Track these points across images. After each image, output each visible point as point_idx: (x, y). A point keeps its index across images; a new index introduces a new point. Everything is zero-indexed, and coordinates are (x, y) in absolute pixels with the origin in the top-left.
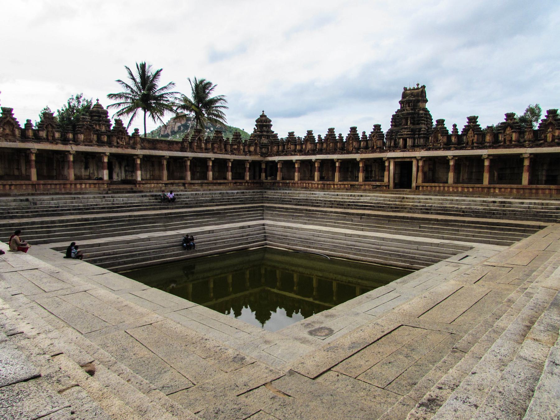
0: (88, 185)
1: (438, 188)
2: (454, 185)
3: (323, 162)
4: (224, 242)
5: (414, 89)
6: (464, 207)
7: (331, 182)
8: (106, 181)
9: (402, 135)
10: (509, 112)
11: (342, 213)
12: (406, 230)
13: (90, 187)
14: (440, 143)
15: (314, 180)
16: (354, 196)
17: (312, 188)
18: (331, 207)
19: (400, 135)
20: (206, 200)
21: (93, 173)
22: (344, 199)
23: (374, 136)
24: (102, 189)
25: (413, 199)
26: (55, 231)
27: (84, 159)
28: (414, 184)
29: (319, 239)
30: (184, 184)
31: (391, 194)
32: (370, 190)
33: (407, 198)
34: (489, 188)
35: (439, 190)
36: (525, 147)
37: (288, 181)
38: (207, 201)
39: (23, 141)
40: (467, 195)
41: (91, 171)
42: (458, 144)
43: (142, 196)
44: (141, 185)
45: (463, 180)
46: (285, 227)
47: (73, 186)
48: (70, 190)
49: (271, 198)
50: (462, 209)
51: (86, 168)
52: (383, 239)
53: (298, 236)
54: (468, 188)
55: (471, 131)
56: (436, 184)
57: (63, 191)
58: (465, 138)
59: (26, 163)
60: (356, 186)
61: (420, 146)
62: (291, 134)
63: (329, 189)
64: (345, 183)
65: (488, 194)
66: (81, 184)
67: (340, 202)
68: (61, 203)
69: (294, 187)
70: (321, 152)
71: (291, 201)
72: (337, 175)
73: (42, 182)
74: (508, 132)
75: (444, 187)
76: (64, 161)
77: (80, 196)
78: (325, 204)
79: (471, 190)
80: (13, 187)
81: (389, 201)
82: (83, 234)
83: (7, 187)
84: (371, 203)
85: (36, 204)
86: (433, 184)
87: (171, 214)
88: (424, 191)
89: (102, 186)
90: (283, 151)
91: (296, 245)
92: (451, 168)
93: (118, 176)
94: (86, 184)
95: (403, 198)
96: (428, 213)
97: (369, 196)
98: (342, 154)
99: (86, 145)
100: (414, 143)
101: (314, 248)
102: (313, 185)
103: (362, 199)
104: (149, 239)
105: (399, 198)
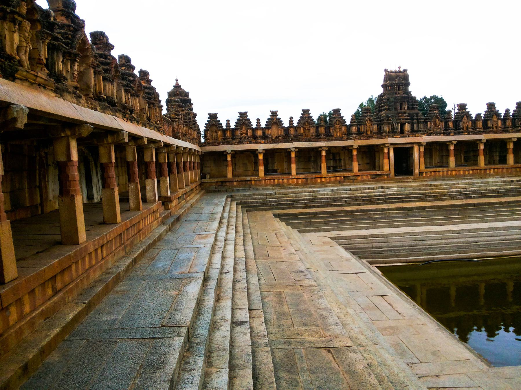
1: (441, 173)
2: (457, 168)
3: (300, 151)
5: (396, 72)
6: (495, 188)
7: (318, 175)
9: (400, 119)
10: (491, 101)
11: (397, 209)
12: (487, 217)
14: (440, 129)
15: (290, 174)
16: (373, 188)
17: (289, 184)
18: (359, 204)
19: (397, 120)
22: (364, 193)
23: (367, 120)
25: (441, 185)
28: (417, 171)
29: (429, 242)
31: (397, 182)
32: (369, 181)
33: (434, 185)
34: (486, 169)
35: (443, 175)
36: (509, 133)
37: (249, 178)
40: (471, 177)
42: (456, 129)
45: (435, 163)
46: (365, 237)
49: (251, 203)
50: (493, 190)
52: (496, 229)
53: (398, 244)
54: (468, 170)
55: (465, 118)
56: (441, 169)
58: (461, 123)
60: (351, 178)
61: (420, 131)
62: (243, 115)
63: (314, 184)
64: (337, 174)
65: (486, 175)
67: (362, 197)
69: (260, 185)
70: (297, 138)
71: (293, 204)
72: (324, 166)
74: (495, 119)
75: (447, 171)
78: (346, 201)
79: (471, 172)
81: (420, 190)
84: (402, 194)
86: (438, 169)
88: (429, 177)
90: (233, 139)
91: (410, 255)
92: (452, 153)
95: (431, 186)
96: (470, 198)
97: (391, 187)
98: (328, 140)
100: (412, 128)
101: (436, 254)
102: (291, 181)
103: (388, 191)
105: (426, 186)
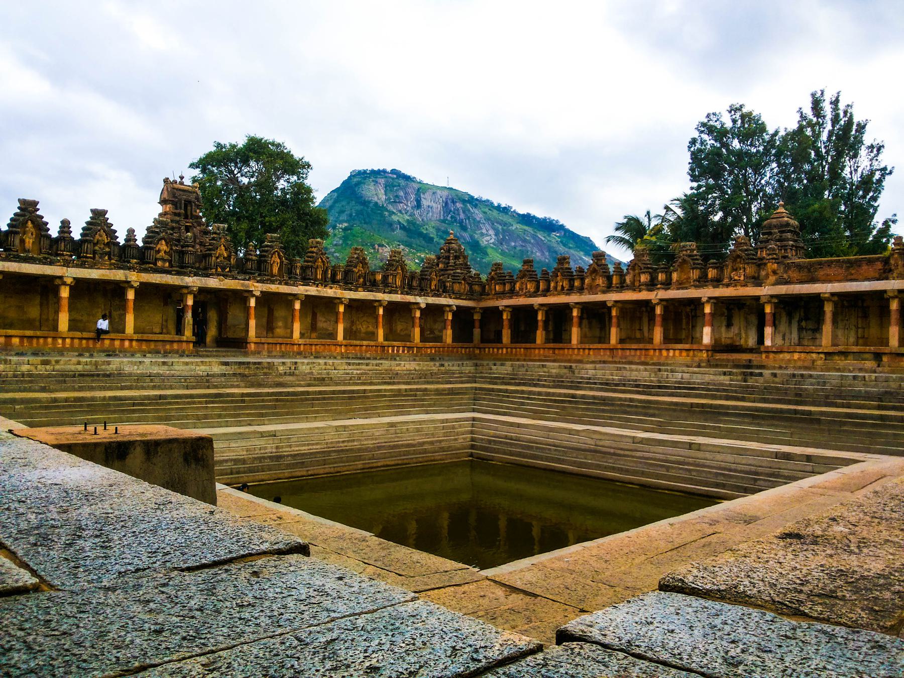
0: (677, 352)
4: (689, 470)
8: (706, 346)
13: (680, 355)
20: (866, 392)
21: (740, 334)
24: (696, 359)
26: (528, 404)
27: (726, 311)
30: (878, 357)
38: (858, 396)
39: (604, 292)
41: (736, 332)
43: (725, 374)
44: (771, 356)
47: (657, 353)
48: (652, 359)
51: (729, 325)
57: (643, 359)
59: (649, 321)
66: (668, 350)
68: (599, 374)
73: (619, 346)
76: (695, 317)
77: (627, 366)
80: (591, 353)
82: (548, 412)
83: (587, 351)
85: (573, 372)
87: (703, 405)
89: (699, 354)
93: (784, 339)
94: (674, 350)
99: (678, 289)
104: (577, 432)
